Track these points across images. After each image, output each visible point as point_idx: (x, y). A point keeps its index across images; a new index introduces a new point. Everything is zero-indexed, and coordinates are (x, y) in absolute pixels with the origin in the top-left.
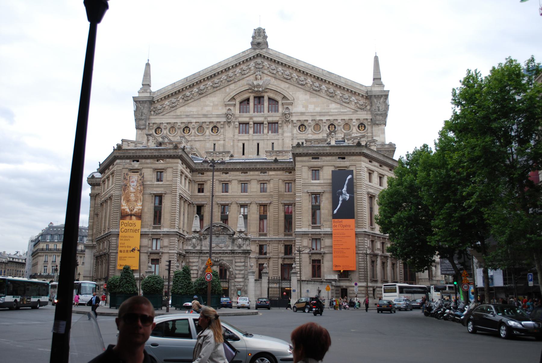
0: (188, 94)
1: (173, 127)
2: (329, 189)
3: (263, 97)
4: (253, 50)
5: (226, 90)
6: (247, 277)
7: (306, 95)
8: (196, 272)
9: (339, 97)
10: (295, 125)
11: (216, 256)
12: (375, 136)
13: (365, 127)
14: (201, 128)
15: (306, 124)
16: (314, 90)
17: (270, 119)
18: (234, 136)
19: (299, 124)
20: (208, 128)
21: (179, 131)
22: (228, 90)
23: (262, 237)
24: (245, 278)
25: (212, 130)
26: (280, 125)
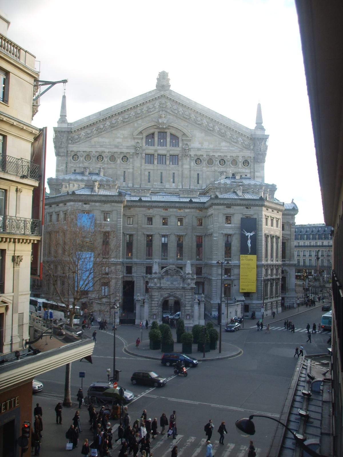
0: (102, 126)
1: (88, 156)
2: (238, 232)
3: (166, 132)
4: (158, 91)
6: (194, 306)
7: (202, 133)
8: (157, 302)
10: (192, 159)
11: (171, 291)
12: (257, 172)
13: (248, 163)
14: (113, 158)
16: (208, 129)
17: (172, 153)
18: (141, 165)
19: (196, 158)
20: (119, 158)
21: (94, 159)
22: (136, 125)
23: (179, 261)
24: (192, 306)
25: (122, 159)
26: (180, 158)
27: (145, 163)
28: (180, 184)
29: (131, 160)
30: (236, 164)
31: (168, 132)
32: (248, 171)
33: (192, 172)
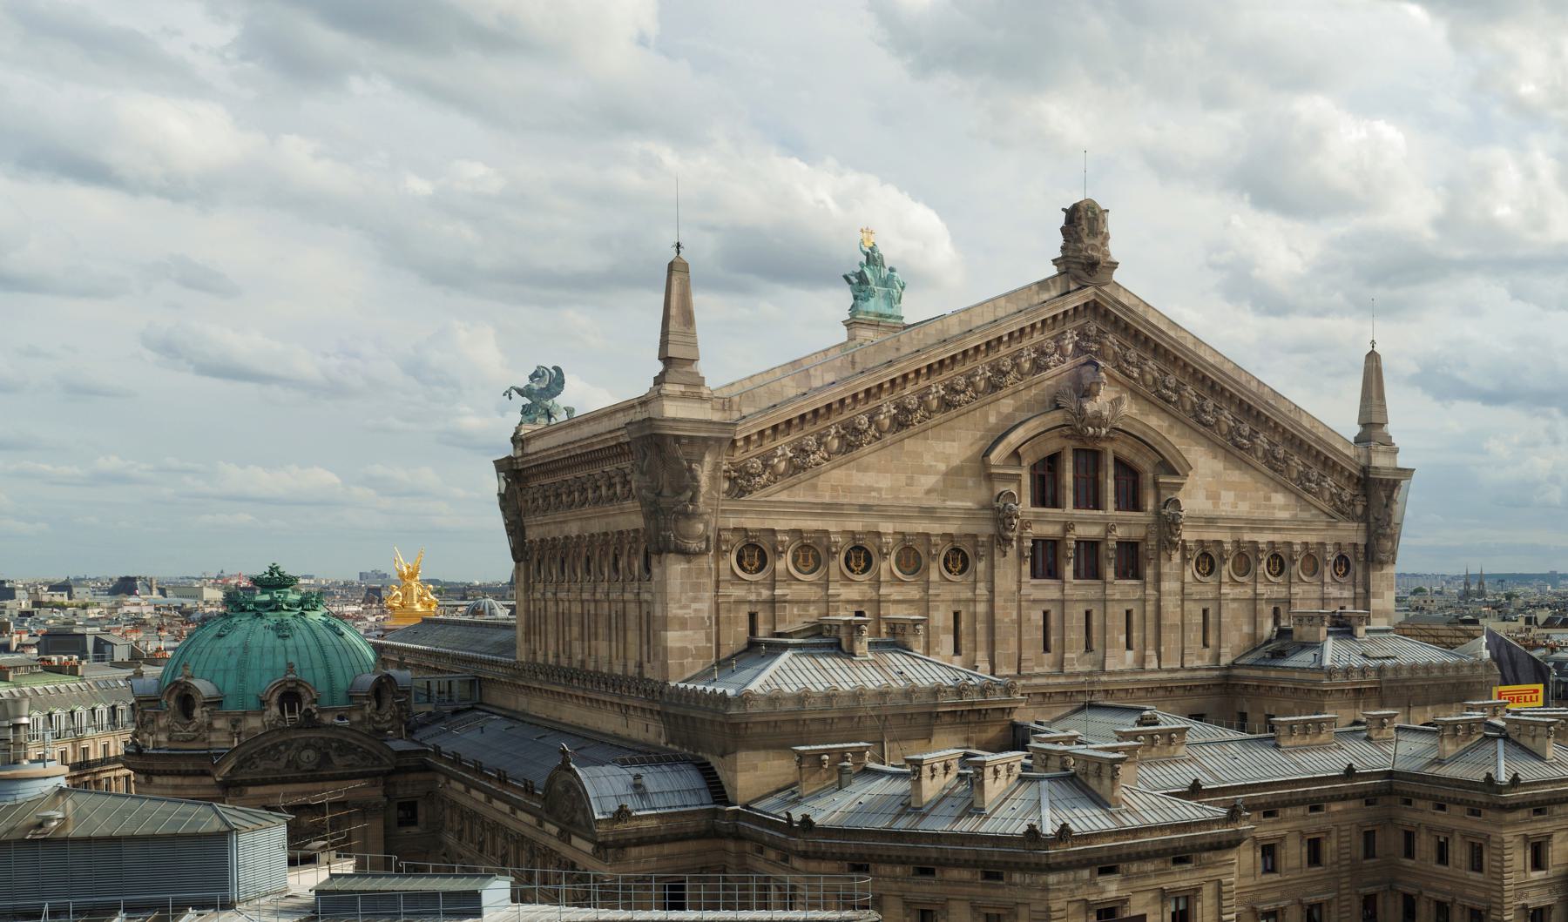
4: (1073, 287)
5: (986, 416)
9: (1295, 475)
15: (1214, 552)
17: (1120, 532)
20: (934, 557)
27: (1034, 575)
31: (1110, 449)
32: (1347, 594)
33: (1189, 605)
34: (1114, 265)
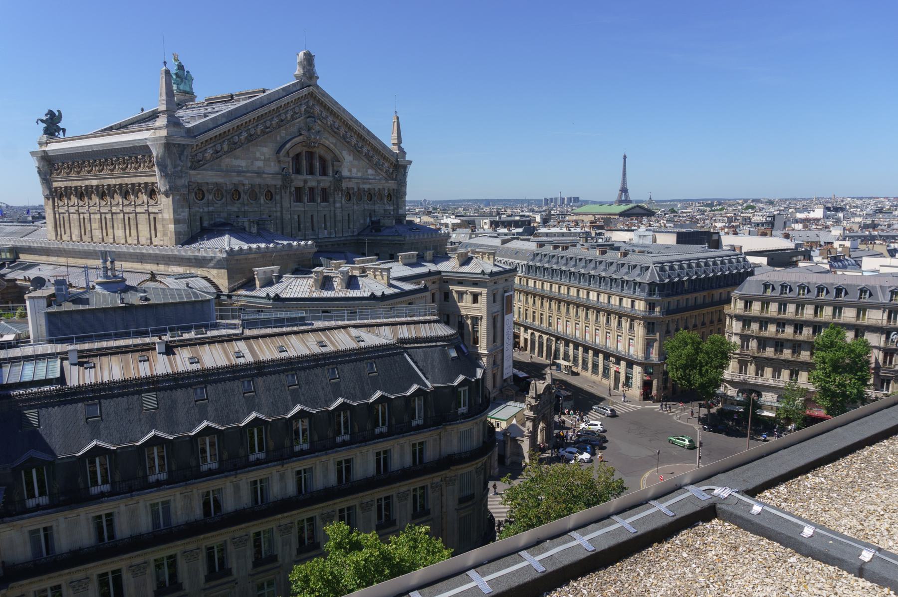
1: (218, 190)
14: (253, 194)
15: (351, 192)
22: (278, 138)
28: (333, 231)
29: (278, 197)
30: (381, 199)
34: (318, 78)
